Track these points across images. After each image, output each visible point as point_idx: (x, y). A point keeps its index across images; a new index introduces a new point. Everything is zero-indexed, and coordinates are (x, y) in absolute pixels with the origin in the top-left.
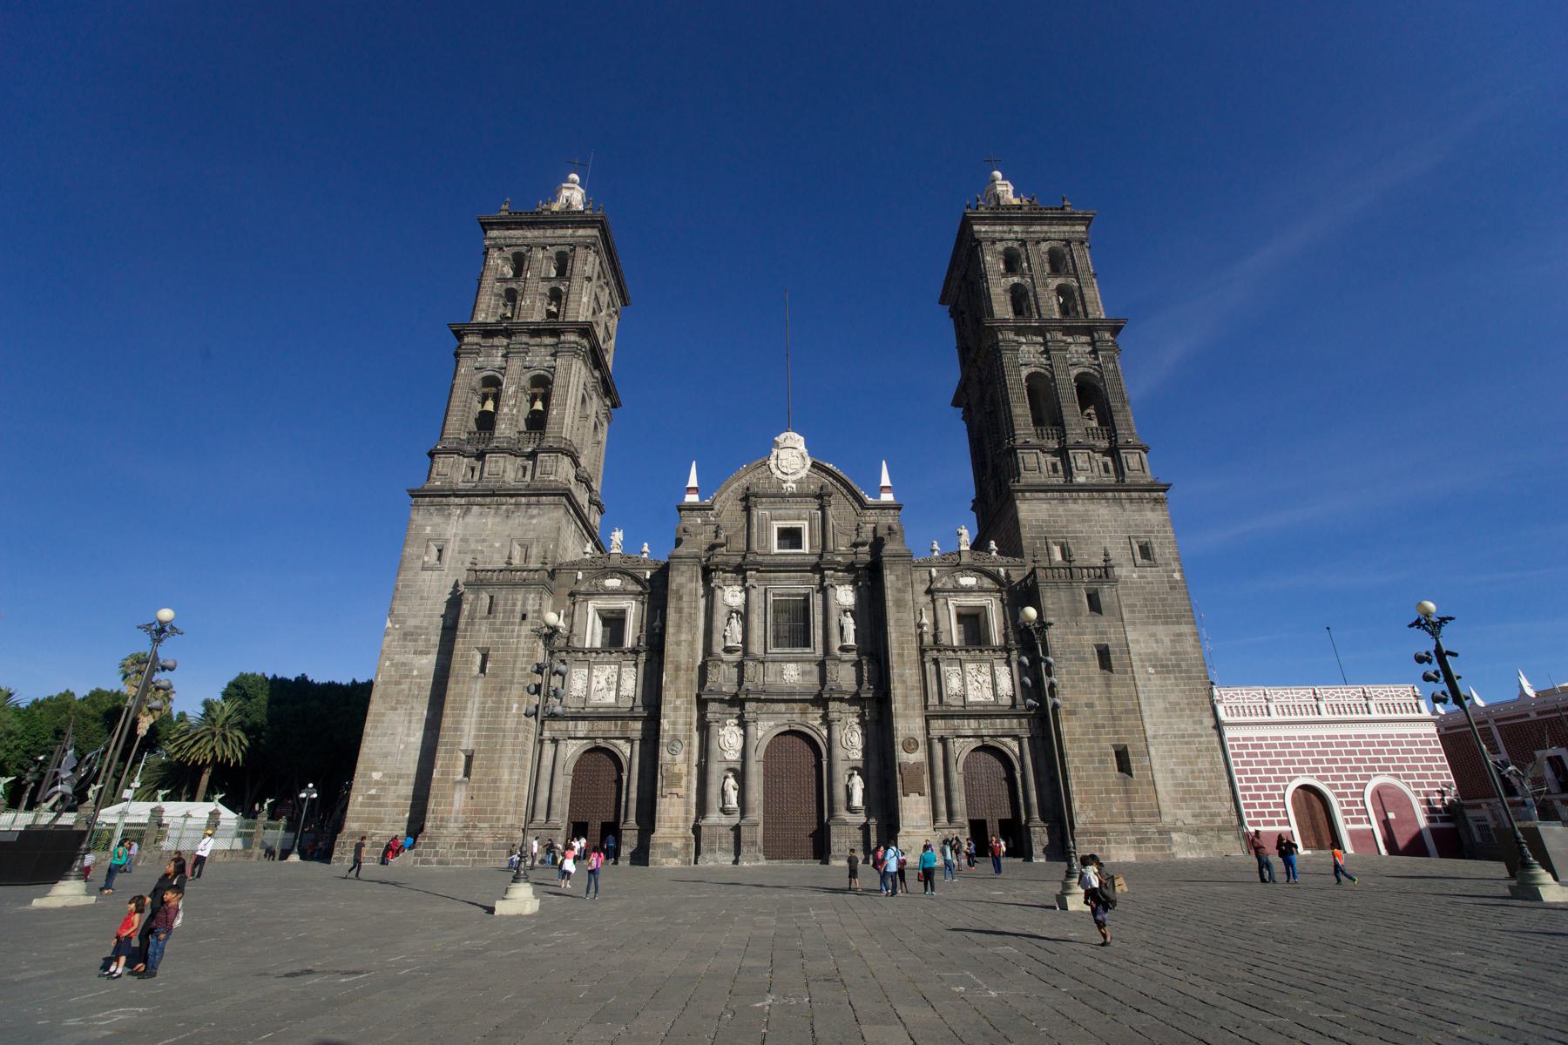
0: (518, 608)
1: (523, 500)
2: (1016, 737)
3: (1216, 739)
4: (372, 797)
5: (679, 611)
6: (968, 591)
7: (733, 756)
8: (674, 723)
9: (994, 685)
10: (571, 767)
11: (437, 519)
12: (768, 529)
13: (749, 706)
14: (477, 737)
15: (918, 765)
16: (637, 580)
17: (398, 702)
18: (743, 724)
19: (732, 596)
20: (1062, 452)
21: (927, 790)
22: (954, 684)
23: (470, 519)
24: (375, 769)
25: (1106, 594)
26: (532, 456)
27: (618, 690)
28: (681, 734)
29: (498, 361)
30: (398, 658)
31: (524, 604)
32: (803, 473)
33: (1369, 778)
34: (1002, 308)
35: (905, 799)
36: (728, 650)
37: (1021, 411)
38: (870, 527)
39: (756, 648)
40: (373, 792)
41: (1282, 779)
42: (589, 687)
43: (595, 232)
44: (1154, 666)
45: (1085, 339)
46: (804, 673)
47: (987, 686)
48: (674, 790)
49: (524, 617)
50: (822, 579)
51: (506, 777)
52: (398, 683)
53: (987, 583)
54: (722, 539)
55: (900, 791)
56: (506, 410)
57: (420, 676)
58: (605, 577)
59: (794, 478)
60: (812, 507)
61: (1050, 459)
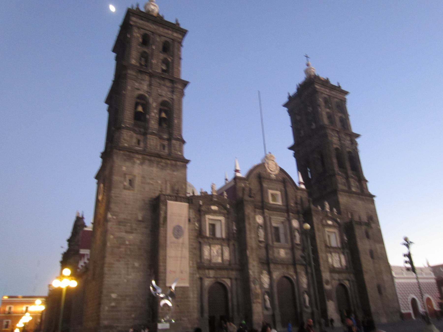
1: (169, 162)
2: (349, 280)
4: (113, 307)
5: (250, 224)
6: (329, 226)
7: (266, 286)
9: (340, 261)
11: (128, 164)
12: (267, 193)
13: (272, 266)
16: (225, 208)
17: (121, 257)
18: (270, 273)
19: (259, 220)
20: (347, 178)
22: (330, 260)
23: (145, 167)
24: (113, 292)
25: (370, 233)
26: (169, 140)
28: (257, 277)
29: (145, 87)
30: (118, 234)
32: (277, 172)
34: (326, 121)
36: (260, 242)
37: (335, 161)
38: (299, 197)
39: (270, 243)
40: (113, 304)
42: (210, 255)
43: (180, 36)
45: (348, 138)
46: (286, 253)
47: (338, 262)
49: (189, 220)
50: (289, 216)
51: (191, 296)
52: (119, 248)
53: (336, 224)
54: (252, 195)
55: (326, 299)
56: (153, 114)
57: (130, 245)
60: (281, 186)
61: (344, 181)
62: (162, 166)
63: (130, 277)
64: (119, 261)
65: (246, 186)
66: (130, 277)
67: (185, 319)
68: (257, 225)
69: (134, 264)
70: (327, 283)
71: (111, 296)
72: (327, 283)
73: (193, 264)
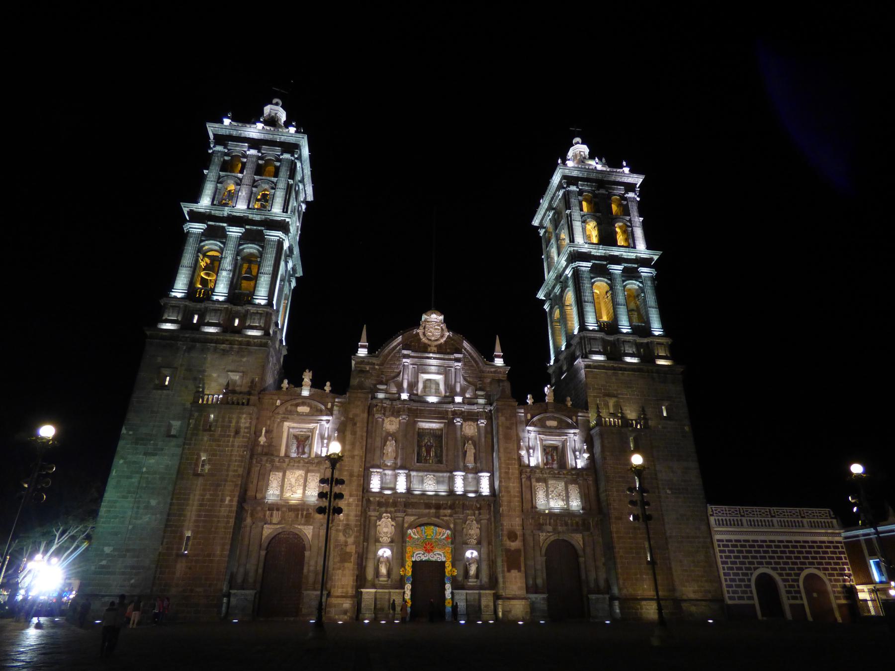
0: (233, 424)
3: (709, 540)
4: (103, 567)
8: (348, 515)
10: (265, 545)
14: (196, 521)
15: (518, 551)
17: (129, 492)
21: (523, 569)
27: (304, 490)
30: (130, 458)
31: (238, 422)
32: (442, 341)
33: (802, 569)
35: (507, 574)
40: (104, 563)
41: (749, 569)
44: (670, 489)
48: (347, 565)
57: (147, 473)
58: (297, 405)
59: (436, 343)
62: (223, 350)
63: (139, 522)
64: (124, 497)
65: (374, 369)
66: (139, 522)
67: (199, 590)
68: (384, 434)
69: (149, 502)
70: (512, 536)
71: (103, 551)
72: (512, 536)
73: (231, 501)
